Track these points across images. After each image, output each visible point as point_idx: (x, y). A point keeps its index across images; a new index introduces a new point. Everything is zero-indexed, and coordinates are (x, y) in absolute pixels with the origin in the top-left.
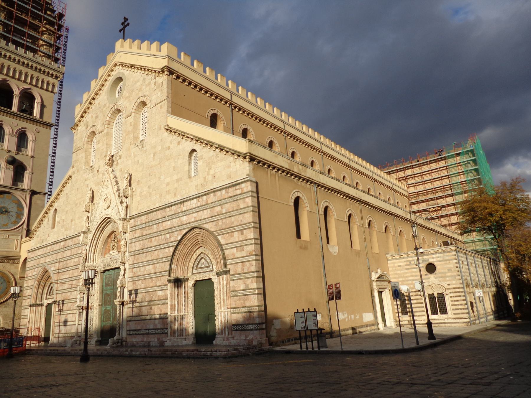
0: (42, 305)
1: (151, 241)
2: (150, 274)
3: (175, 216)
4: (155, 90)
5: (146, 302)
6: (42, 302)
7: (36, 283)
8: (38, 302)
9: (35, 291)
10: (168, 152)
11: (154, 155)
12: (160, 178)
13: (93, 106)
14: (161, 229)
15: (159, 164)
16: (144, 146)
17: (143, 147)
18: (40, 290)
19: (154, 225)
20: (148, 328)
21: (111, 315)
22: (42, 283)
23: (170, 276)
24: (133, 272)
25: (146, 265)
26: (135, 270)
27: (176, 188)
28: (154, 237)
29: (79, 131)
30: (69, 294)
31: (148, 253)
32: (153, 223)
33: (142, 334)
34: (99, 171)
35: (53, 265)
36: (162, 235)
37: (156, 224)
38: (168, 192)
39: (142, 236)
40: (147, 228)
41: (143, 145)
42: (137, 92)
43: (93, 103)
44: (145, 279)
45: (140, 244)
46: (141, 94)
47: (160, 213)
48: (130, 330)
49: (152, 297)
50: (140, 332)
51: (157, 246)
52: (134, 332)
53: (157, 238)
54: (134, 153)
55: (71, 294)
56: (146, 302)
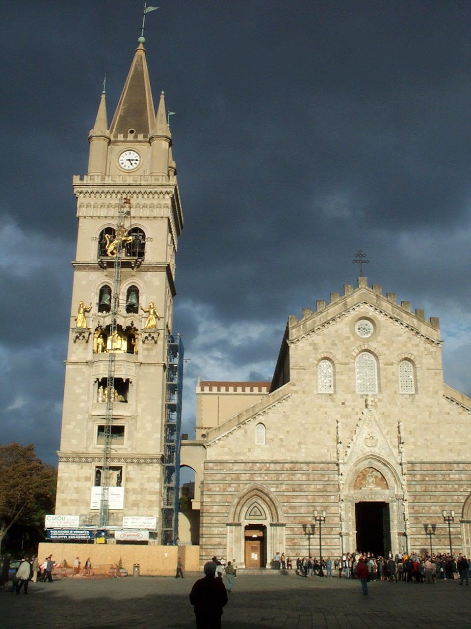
0: (240, 525)
3: (464, 472)
4: (426, 355)
6: (240, 522)
7: (236, 500)
8: (236, 521)
9: (233, 509)
10: (447, 416)
11: (430, 413)
13: (325, 331)
14: (448, 479)
15: (438, 423)
16: (415, 400)
18: (239, 508)
22: (243, 501)
23: (462, 517)
24: (413, 509)
27: (460, 450)
29: (299, 348)
34: (346, 404)
35: (274, 485)
36: (449, 484)
38: (451, 451)
40: (429, 475)
41: (413, 399)
42: (400, 346)
43: (326, 327)
46: (404, 349)
47: (446, 466)
49: (441, 532)
53: (443, 486)
54: (401, 403)
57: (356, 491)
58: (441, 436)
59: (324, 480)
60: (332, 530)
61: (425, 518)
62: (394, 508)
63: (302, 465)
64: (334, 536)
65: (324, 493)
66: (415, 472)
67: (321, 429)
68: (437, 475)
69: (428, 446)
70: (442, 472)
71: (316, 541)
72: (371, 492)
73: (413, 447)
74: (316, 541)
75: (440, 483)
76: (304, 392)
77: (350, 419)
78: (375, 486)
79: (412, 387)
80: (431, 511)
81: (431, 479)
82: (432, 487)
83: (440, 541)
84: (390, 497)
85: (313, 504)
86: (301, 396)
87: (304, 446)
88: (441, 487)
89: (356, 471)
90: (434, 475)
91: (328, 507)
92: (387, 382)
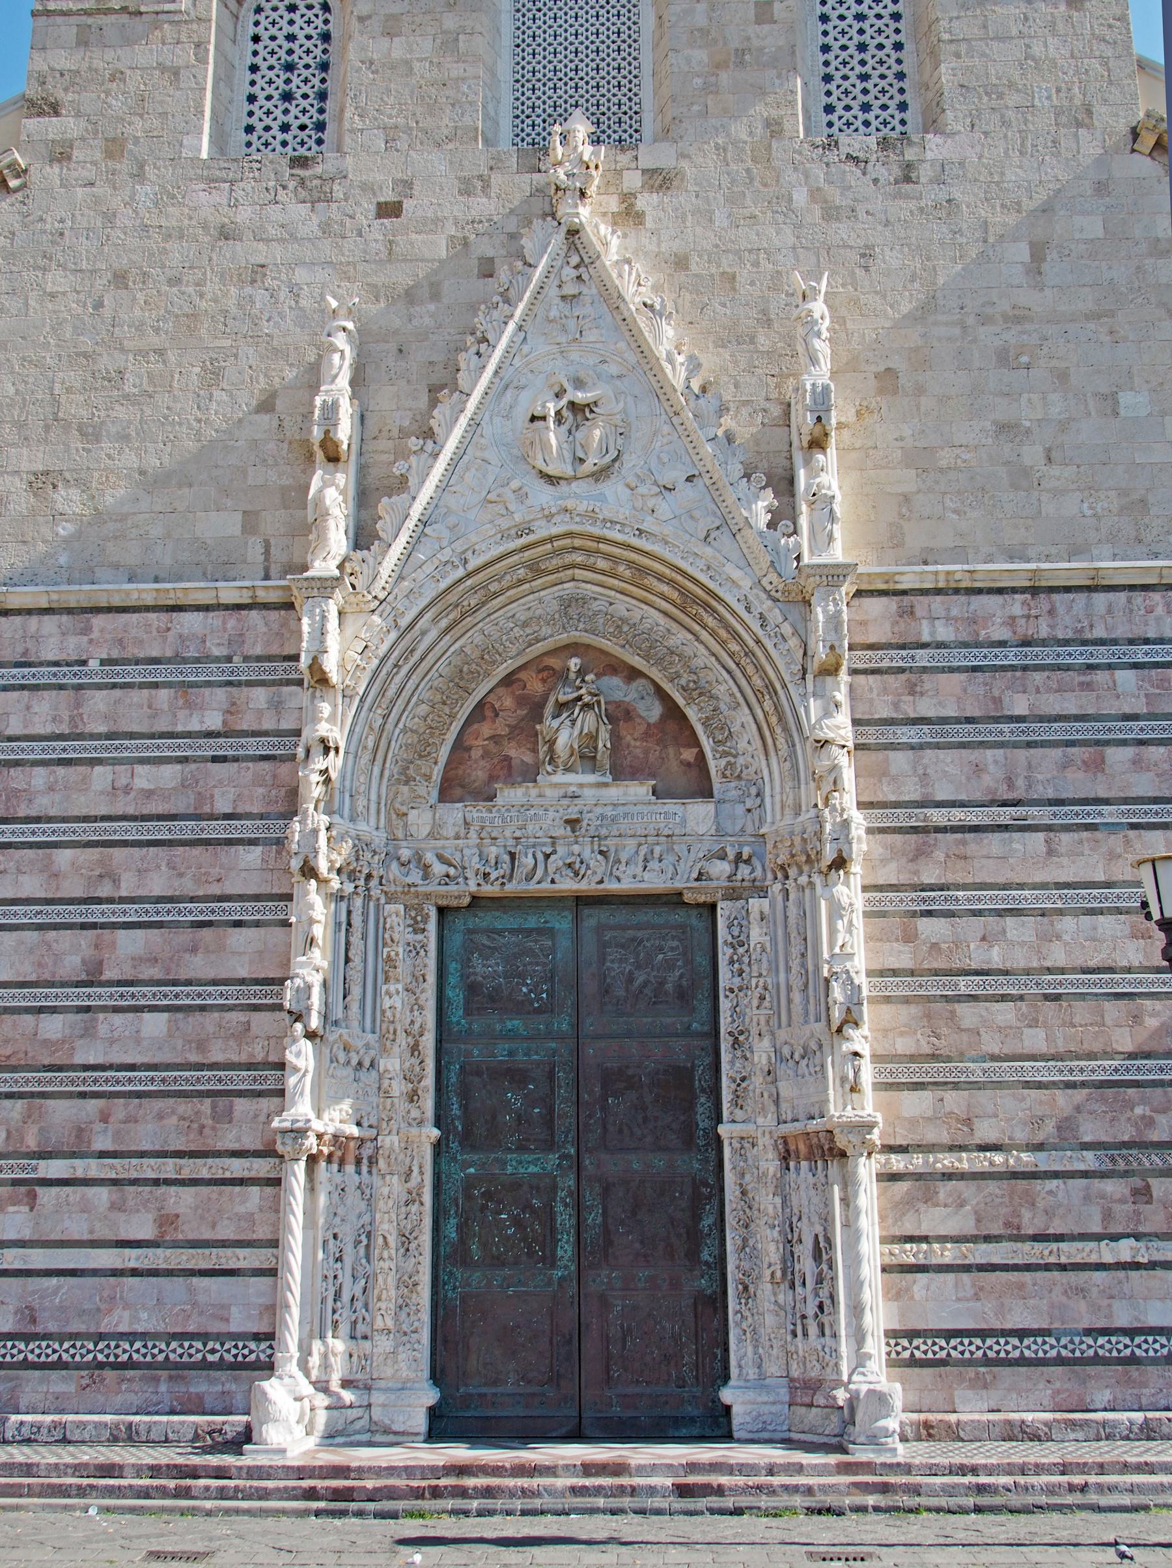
1: (1097, 766)
2: (1111, 970)
5: (1086, 1146)
12: (1110, 400)
16: (925, 173)
17: (907, 179)
19: (1110, 667)
20: (1122, 1321)
21: (564, 1217)
25: (1061, 912)
26: (925, 926)
28: (1124, 743)
30: (53, 1027)
31: (1066, 837)
32: (1102, 655)
33: (1060, 1361)
37: (1136, 666)
39: (997, 720)
40: (1038, 677)
41: (909, 166)
44: (1057, 998)
45: (978, 769)
48: (912, 1334)
49: (1150, 1122)
50: (1050, 1348)
51: (1156, 800)
52: (974, 1348)
54: (815, 194)
55: (88, 1032)
56: (1086, 1146)
57: (454, 814)
58: (1126, 398)
59: (195, 726)
60: (227, 1116)
61: (1005, 1013)
62: (756, 934)
63: (34, 621)
64: (237, 1167)
65: (186, 829)
66: (923, 658)
67: (213, 375)
68: (1101, 677)
69: (1026, 472)
70: (1140, 654)
71: (85, 1208)
72: (573, 823)
73: (908, 481)
74: (85, 1208)
75: (1135, 730)
76: (114, 148)
77: (432, 307)
78: (608, 779)
79: (903, 107)
80: (1058, 956)
81: (1053, 704)
82: (1065, 765)
83: (1143, 1194)
84: (723, 857)
85: (97, 912)
86: (88, 173)
87: (75, 493)
88: (1136, 762)
89: (461, 680)
90: (1077, 678)
91: (206, 932)
92: (720, 65)
